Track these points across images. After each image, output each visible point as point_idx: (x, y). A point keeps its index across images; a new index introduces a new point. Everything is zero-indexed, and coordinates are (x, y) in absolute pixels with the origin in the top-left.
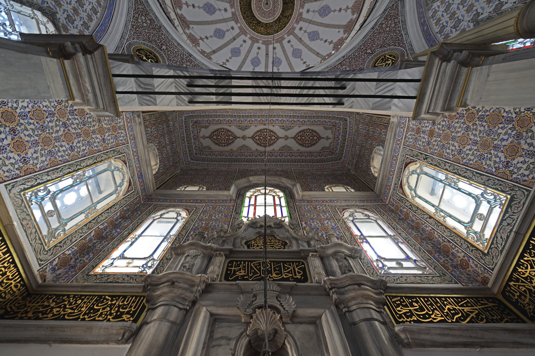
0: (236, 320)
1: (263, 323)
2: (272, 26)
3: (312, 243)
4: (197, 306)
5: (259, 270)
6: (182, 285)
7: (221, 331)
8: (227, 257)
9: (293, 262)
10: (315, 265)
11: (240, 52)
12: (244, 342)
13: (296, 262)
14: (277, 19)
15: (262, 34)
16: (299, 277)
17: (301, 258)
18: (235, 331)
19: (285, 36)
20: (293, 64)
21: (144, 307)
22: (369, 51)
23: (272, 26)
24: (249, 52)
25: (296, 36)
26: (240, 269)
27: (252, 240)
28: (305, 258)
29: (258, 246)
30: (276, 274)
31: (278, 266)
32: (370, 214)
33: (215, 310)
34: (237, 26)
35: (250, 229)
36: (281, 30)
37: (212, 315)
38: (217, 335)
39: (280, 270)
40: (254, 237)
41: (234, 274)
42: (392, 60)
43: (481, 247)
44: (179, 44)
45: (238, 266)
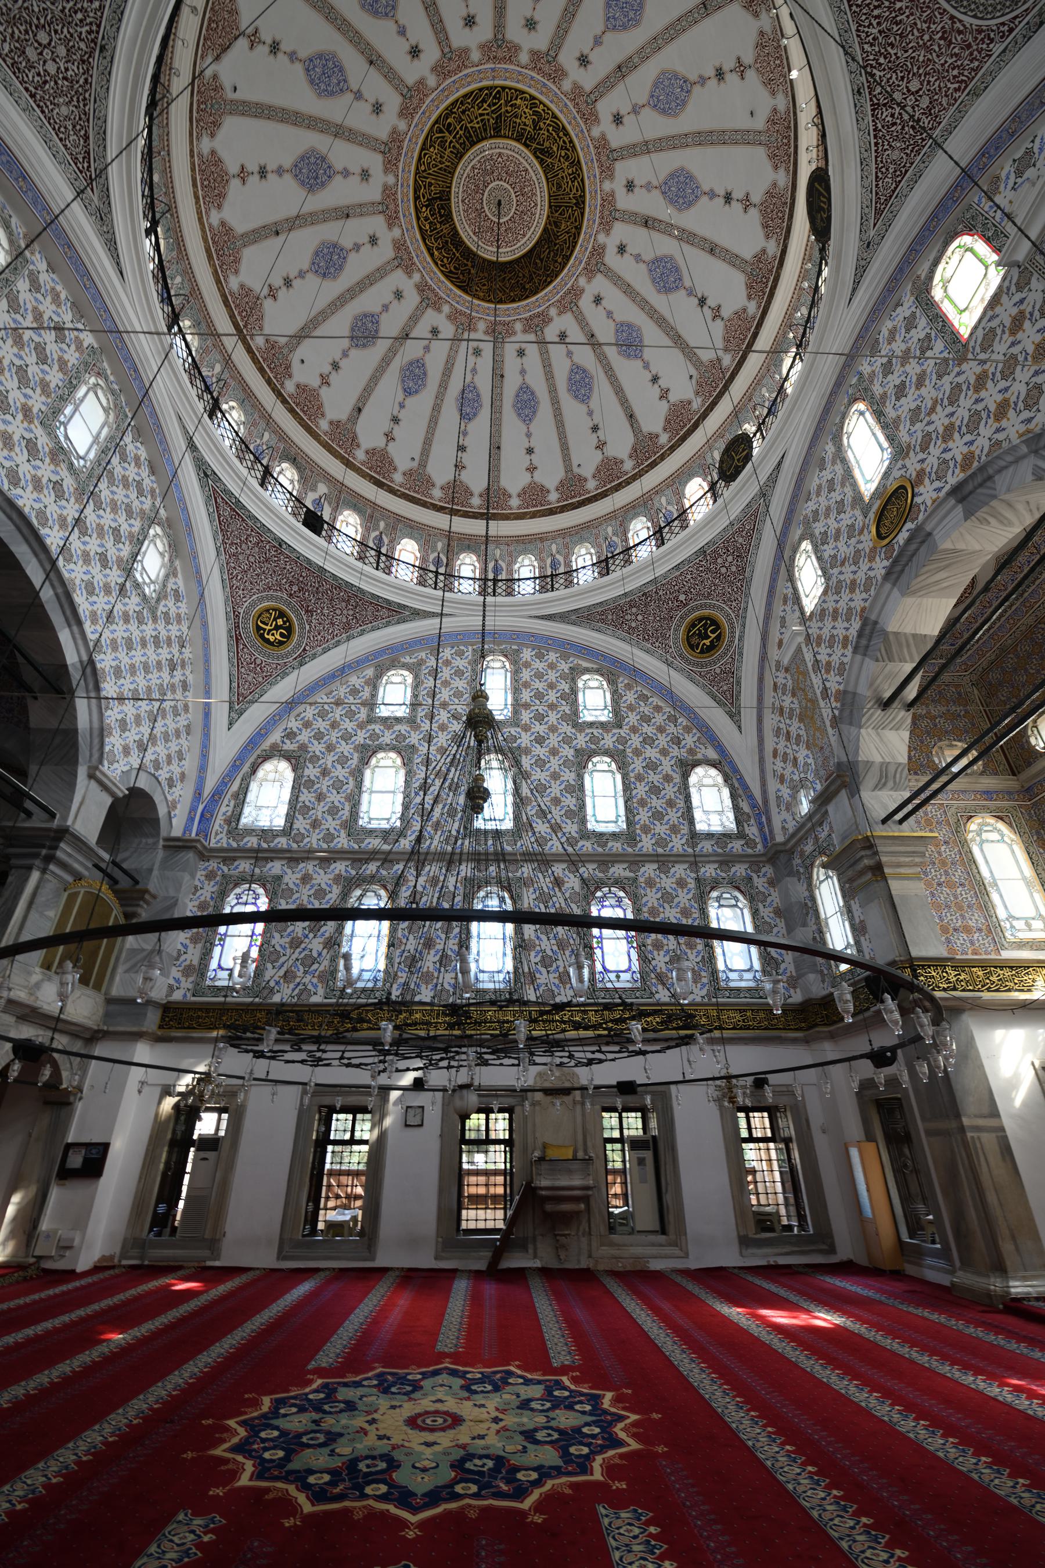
2: (559, 186)
11: (630, 326)
14: (541, 162)
15: (579, 229)
19: (596, 132)
20: (706, 126)
23: (559, 186)
24: (629, 290)
25: (605, 86)
34: (556, 319)
36: (574, 147)
44: (677, 567)
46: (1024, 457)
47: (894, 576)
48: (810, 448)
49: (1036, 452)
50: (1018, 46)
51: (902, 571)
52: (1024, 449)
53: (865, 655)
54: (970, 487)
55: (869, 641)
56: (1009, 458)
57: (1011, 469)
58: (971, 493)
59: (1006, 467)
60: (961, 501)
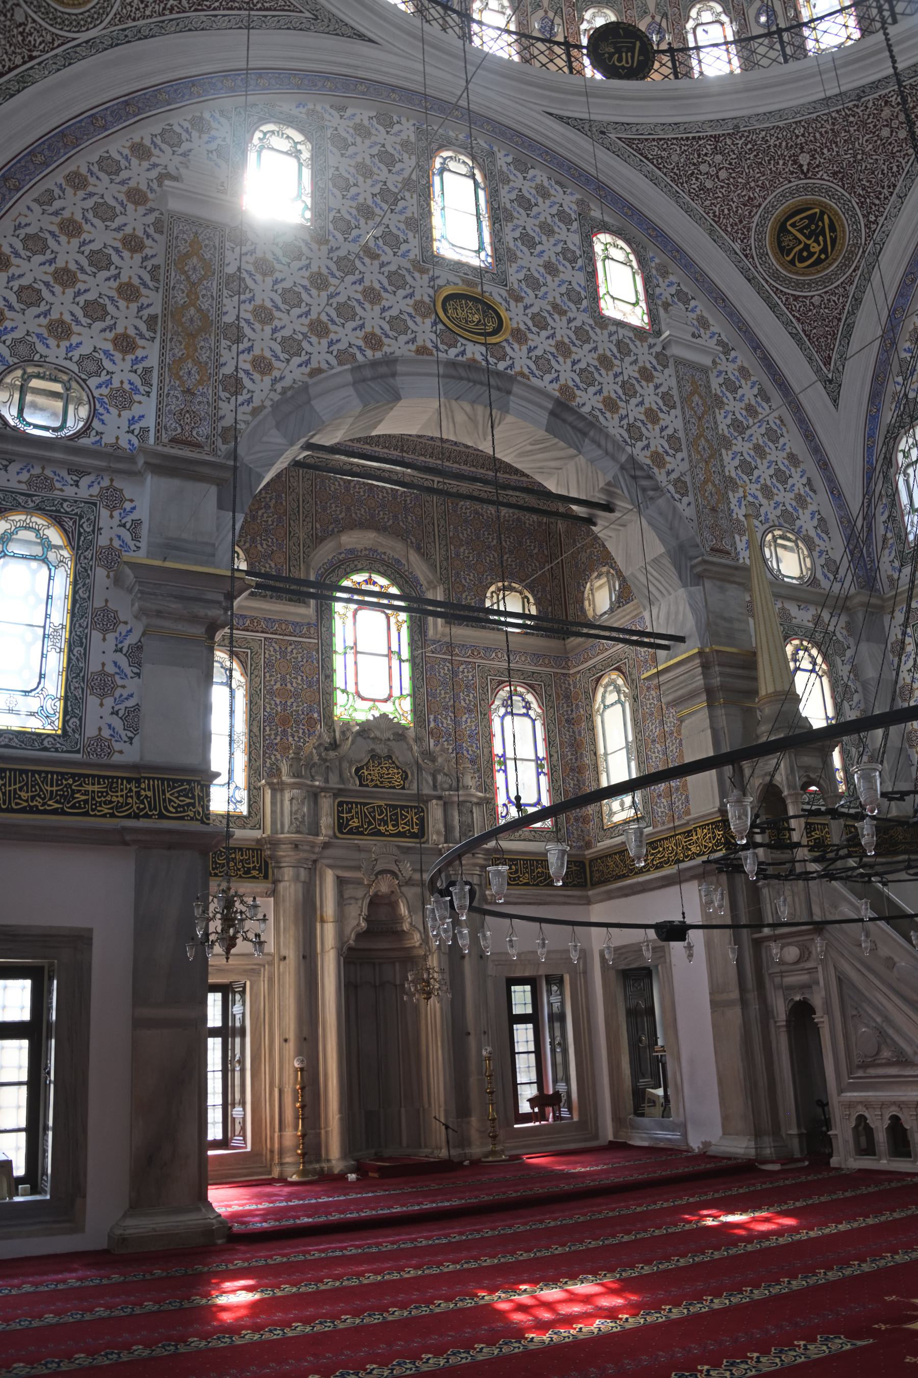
0: (359, 882)
3: (440, 778)
4: (319, 866)
5: (374, 818)
6: (305, 847)
7: (349, 892)
8: (335, 796)
9: (411, 807)
10: (435, 812)
12: (367, 901)
13: (415, 807)
16: (416, 831)
18: (360, 893)
21: (266, 864)
22: (804, 159)
26: (352, 818)
27: (362, 768)
29: (372, 780)
30: (393, 826)
31: (395, 812)
32: (534, 705)
35: (359, 739)
37: (338, 877)
38: (346, 896)
39: (397, 820)
40: (366, 761)
41: (348, 825)
42: (824, 250)
43: (605, 821)
46: (614, 458)
47: (453, 373)
48: (394, 88)
49: (622, 468)
50: (737, 263)
51: (461, 378)
52: (623, 458)
53: (354, 383)
54: (571, 418)
55: (373, 379)
56: (610, 447)
57: (600, 452)
58: (564, 421)
59: (599, 446)
60: (552, 413)
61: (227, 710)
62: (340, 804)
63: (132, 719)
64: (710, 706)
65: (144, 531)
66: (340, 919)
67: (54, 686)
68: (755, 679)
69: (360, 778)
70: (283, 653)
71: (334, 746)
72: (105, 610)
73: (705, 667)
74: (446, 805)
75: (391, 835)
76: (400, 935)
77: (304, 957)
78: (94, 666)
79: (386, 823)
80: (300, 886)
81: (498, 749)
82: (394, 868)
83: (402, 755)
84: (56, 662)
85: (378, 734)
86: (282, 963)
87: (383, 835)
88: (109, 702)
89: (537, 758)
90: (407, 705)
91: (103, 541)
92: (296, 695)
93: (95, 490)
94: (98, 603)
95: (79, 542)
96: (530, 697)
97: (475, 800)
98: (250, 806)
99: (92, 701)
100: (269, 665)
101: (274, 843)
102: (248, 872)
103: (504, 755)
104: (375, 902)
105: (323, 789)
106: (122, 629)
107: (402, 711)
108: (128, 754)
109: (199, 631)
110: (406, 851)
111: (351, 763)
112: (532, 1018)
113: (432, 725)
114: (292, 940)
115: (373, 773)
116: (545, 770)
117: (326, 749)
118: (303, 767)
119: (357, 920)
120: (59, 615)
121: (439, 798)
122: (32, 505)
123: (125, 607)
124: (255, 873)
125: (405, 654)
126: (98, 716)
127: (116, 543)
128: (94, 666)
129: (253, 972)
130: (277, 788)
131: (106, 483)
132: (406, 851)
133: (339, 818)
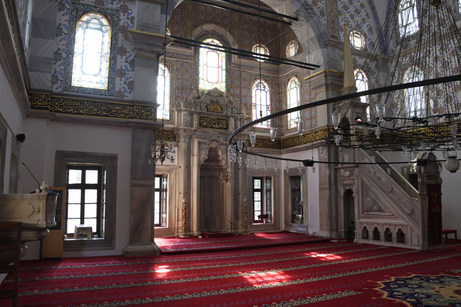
0: (205, 143)
1: (214, 145)
3: (234, 110)
4: (192, 137)
7: (202, 146)
8: (199, 114)
10: (232, 122)
12: (208, 150)
17: (227, 118)
18: (206, 147)
21: (175, 136)
27: (208, 105)
28: (229, 118)
31: (219, 121)
32: (267, 87)
33: (200, 140)
35: (207, 96)
39: (219, 123)
45: (203, 120)
61: (163, 84)
62: (200, 117)
63: (131, 85)
64: (327, 90)
65: (135, 21)
66: (199, 155)
67: (105, 73)
68: (343, 82)
69: (207, 109)
70: (182, 66)
71: (199, 98)
72: (122, 48)
73: (326, 76)
74: (236, 119)
75: (217, 128)
76: (218, 161)
77: (187, 167)
78: (118, 67)
79: (215, 124)
80: (186, 144)
81: (254, 101)
82: (218, 139)
83: (221, 102)
84: (106, 65)
85: (214, 94)
86: (180, 169)
87: (214, 128)
88: (123, 79)
89: (267, 105)
90: (224, 85)
91: (121, 24)
92: (186, 80)
93: (118, 6)
94: (120, 45)
95: (113, 24)
96: (265, 84)
97: (245, 118)
98: (170, 117)
99: (118, 79)
100: (177, 69)
101: (178, 129)
102: (169, 138)
103: (256, 104)
104: (211, 150)
105: (195, 112)
106: (128, 54)
107: (222, 87)
108: (130, 97)
109: (154, 56)
110: (222, 134)
111: (204, 103)
112: (260, 190)
113: (232, 92)
114: (183, 161)
115: (212, 107)
116: (269, 109)
117: (196, 99)
118: (188, 104)
119: (205, 155)
120: (107, 49)
121: (233, 117)
122: (97, 10)
123: (129, 47)
124: (171, 139)
125: (224, 67)
126: (119, 84)
127: (126, 25)
128: (118, 67)
129: (170, 171)
130: (179, 111)
131: (122, 3)
132: (222, 134)
133: (200, 122)
